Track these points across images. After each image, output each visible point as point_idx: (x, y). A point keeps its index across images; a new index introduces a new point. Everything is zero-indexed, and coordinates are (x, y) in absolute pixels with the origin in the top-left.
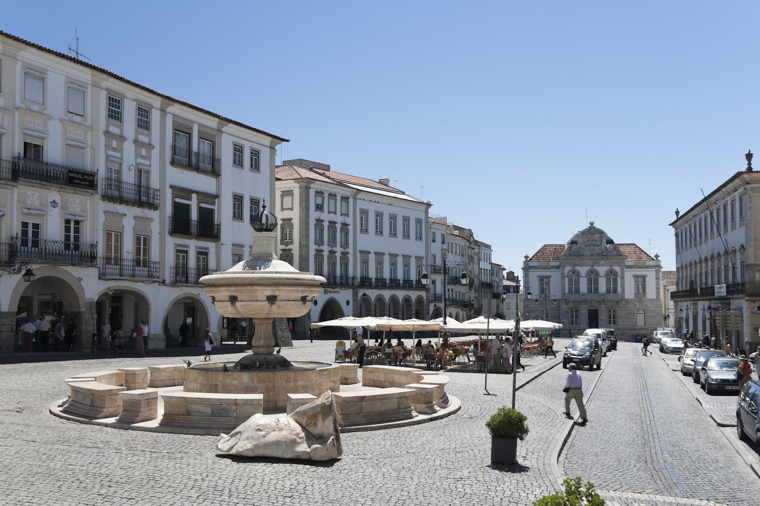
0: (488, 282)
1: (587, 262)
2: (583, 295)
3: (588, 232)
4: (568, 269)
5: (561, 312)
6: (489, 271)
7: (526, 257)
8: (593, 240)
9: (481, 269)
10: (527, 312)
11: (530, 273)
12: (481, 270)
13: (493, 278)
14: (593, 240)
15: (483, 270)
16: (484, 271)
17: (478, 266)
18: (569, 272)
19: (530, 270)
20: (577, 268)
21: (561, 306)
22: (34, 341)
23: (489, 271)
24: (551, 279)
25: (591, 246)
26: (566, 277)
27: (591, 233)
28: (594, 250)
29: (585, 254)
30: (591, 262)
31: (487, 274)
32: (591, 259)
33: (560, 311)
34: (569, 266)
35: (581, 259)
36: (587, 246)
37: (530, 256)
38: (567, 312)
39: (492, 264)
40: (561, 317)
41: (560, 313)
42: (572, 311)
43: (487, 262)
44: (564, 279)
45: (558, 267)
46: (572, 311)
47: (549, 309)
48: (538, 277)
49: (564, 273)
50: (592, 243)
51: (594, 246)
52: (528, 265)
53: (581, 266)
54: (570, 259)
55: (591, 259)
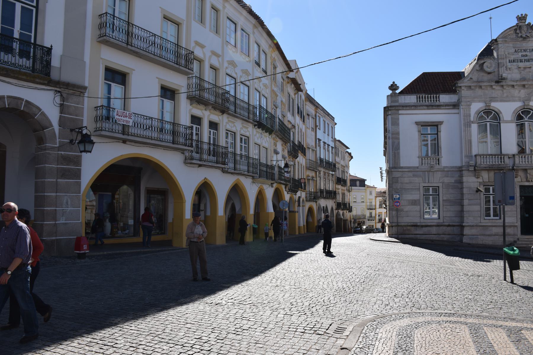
0: (330, 161)
1: (515, 92)
2: (509, 158)
3: (514, 36)
4: (476, 107)
5: (465, 191)
6: (332, 147)
7: (393, 87)
8: (525, 51)
9: (320, 140)
10: (397, 193)
11: (401, 117)
12: (319, 143)
13: (338, 159)
14: (525, 51)
15: (322, 144)
16: (324, 145)
17: (313, 133)
18: (478, 112)
19: (400, 112)
20: (496, 105)
21: (465, 179)
22: (4, 227)
23: (332, 147)
24: (443, 128)
25: (521, 61)
26: (473, 122)
27: (521, 37)
28: (528, 70)
29: (509, 76)
30: (523, 93)
31: (328, 151)
32: (524, 86)
33: (462, 188)
34: (479, 102)
35: (502, 86)
36: (514, 61)
37: (402, 86)
38: (478, 191)
39: (335, 140)
40: (466, 202)
41: (462, 194)
42: (487, 190)
43: (328, 135)
44: (470, 126)
45: (456, 106)
46: (487, 190)
47: (440, 185)
48: (417, 123)
49: (470, 116)
50: (522, 56)
51: (528, 61)
52: (397, 101)
53: (503, 100)
54: (480, 87)
55: (524, 86)
